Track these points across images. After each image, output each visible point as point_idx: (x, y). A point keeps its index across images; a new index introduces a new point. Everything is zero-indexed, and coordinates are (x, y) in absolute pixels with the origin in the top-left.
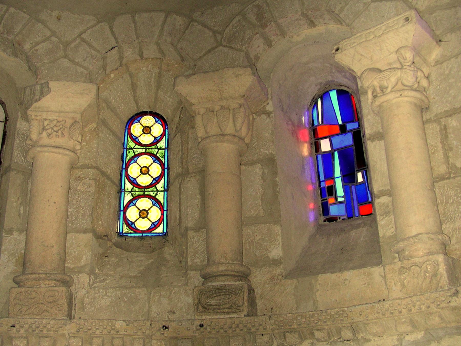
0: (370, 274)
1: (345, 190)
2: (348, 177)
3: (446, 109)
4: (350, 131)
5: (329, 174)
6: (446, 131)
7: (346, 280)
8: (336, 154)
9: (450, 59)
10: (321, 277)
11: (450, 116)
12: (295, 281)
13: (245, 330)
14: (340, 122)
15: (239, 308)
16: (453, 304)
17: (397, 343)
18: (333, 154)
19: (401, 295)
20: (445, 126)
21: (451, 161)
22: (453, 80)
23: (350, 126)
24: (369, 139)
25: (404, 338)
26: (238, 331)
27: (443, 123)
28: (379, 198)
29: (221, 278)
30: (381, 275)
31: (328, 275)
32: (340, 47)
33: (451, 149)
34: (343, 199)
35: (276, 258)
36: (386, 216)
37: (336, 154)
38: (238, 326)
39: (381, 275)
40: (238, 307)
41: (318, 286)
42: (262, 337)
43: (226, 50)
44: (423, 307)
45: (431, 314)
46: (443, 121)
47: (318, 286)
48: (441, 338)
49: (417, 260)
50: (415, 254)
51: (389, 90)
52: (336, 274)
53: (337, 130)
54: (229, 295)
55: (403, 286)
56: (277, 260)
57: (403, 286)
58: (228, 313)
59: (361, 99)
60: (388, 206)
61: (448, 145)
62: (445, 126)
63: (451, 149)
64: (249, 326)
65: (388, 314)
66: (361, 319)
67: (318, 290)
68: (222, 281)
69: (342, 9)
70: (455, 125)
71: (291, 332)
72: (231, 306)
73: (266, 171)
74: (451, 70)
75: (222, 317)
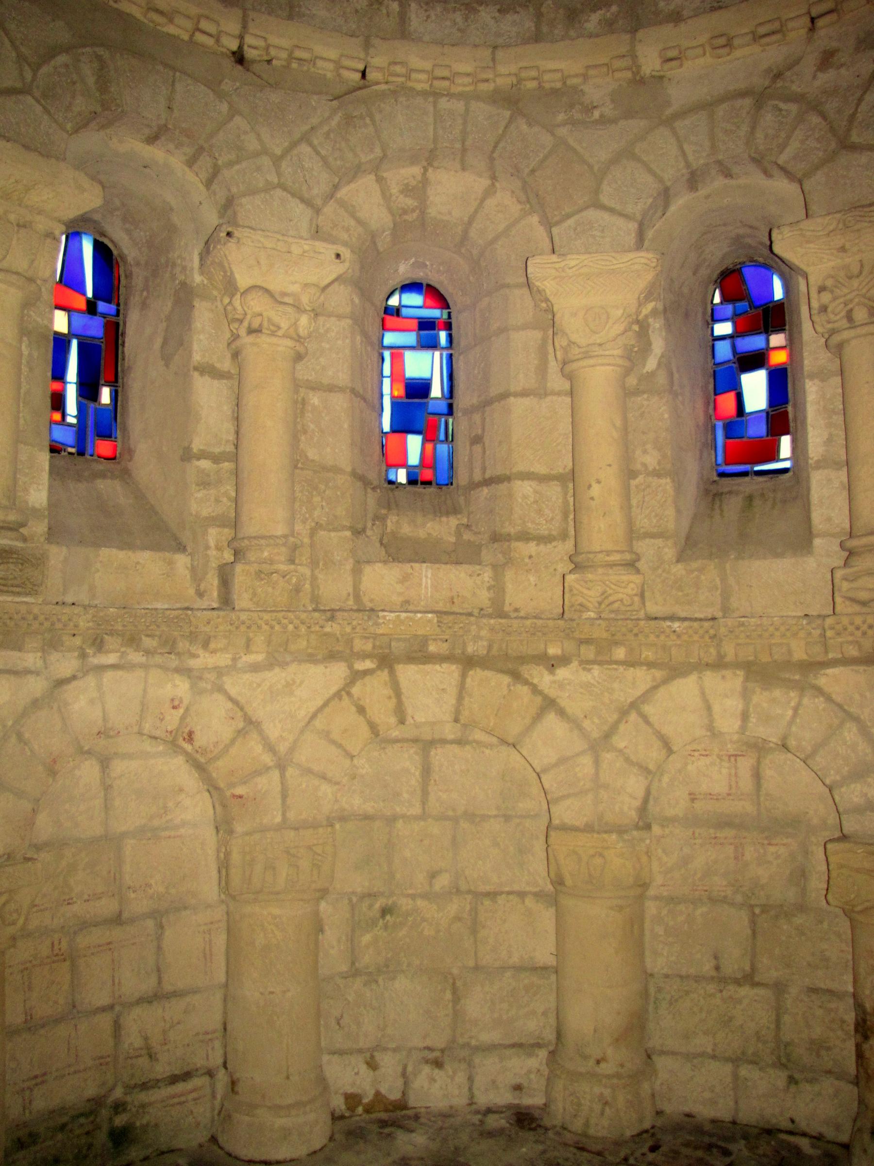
0: (171, 563)
1: (81, 408)
2: (88, 391)
3: (310, 378)
4: (104, 315)
5: (59, 373)
6: (303, 408)
7: (138, 563)
8: (74, 344)
9: (329, 316)
10: (105, 553)
11: (313, 389)
12: (64, 549)
13: (47, 624)
14: (90, 294)
15: (36, 588)
16: (328, 629)
17: (230, 663)
18: (69, 342)
19: (251, 606)
20: (303, 399)
21: (302, 446)
22: (327, 346)
23: (102, 306)
24: (196, 369)
25: (240, 658)
26: (36, 625)
27: (302, 395)
28: (199, 459)
29: (9, 533)
30: (187, 568)
31: (114, 551)
32: (236, 234)
33: (305, 432)
34: (74, 421)
35: (37, 506)
36: (204, 488)
37: (74, 344)
38: (36, 618)
39: (187, 568)
40: (35, 585)
41: (98, 565)
42: (72, 638)
43: (38, 109)
44: (291, 627)
45: (299, 636)
46: (302, 391)
47: (98, 565)
48: (287, 664)
49: (282, 567)
50: (277, 558)
51: (280, 333)
52: (124, 552)
53: (83, 305)
54: (22, 564)
55: (255, 594)
56: (40, 510)
57: (255, 594)
58: (19, 594)
59: (195, 303)
60: (208, 475)
61: (303, 425)
62: (303, 399)
63: (305, 432)
64: (54, 618)
65: (243, 628)
66: (207, 629)
67: (98, 571)
68: (12, 539)
69: (230, 164)
70: (316, 403)
71: (112, 635)
72: (23, 583)
73: (35, 354)
74: (327, 331)
75: (10, 599)
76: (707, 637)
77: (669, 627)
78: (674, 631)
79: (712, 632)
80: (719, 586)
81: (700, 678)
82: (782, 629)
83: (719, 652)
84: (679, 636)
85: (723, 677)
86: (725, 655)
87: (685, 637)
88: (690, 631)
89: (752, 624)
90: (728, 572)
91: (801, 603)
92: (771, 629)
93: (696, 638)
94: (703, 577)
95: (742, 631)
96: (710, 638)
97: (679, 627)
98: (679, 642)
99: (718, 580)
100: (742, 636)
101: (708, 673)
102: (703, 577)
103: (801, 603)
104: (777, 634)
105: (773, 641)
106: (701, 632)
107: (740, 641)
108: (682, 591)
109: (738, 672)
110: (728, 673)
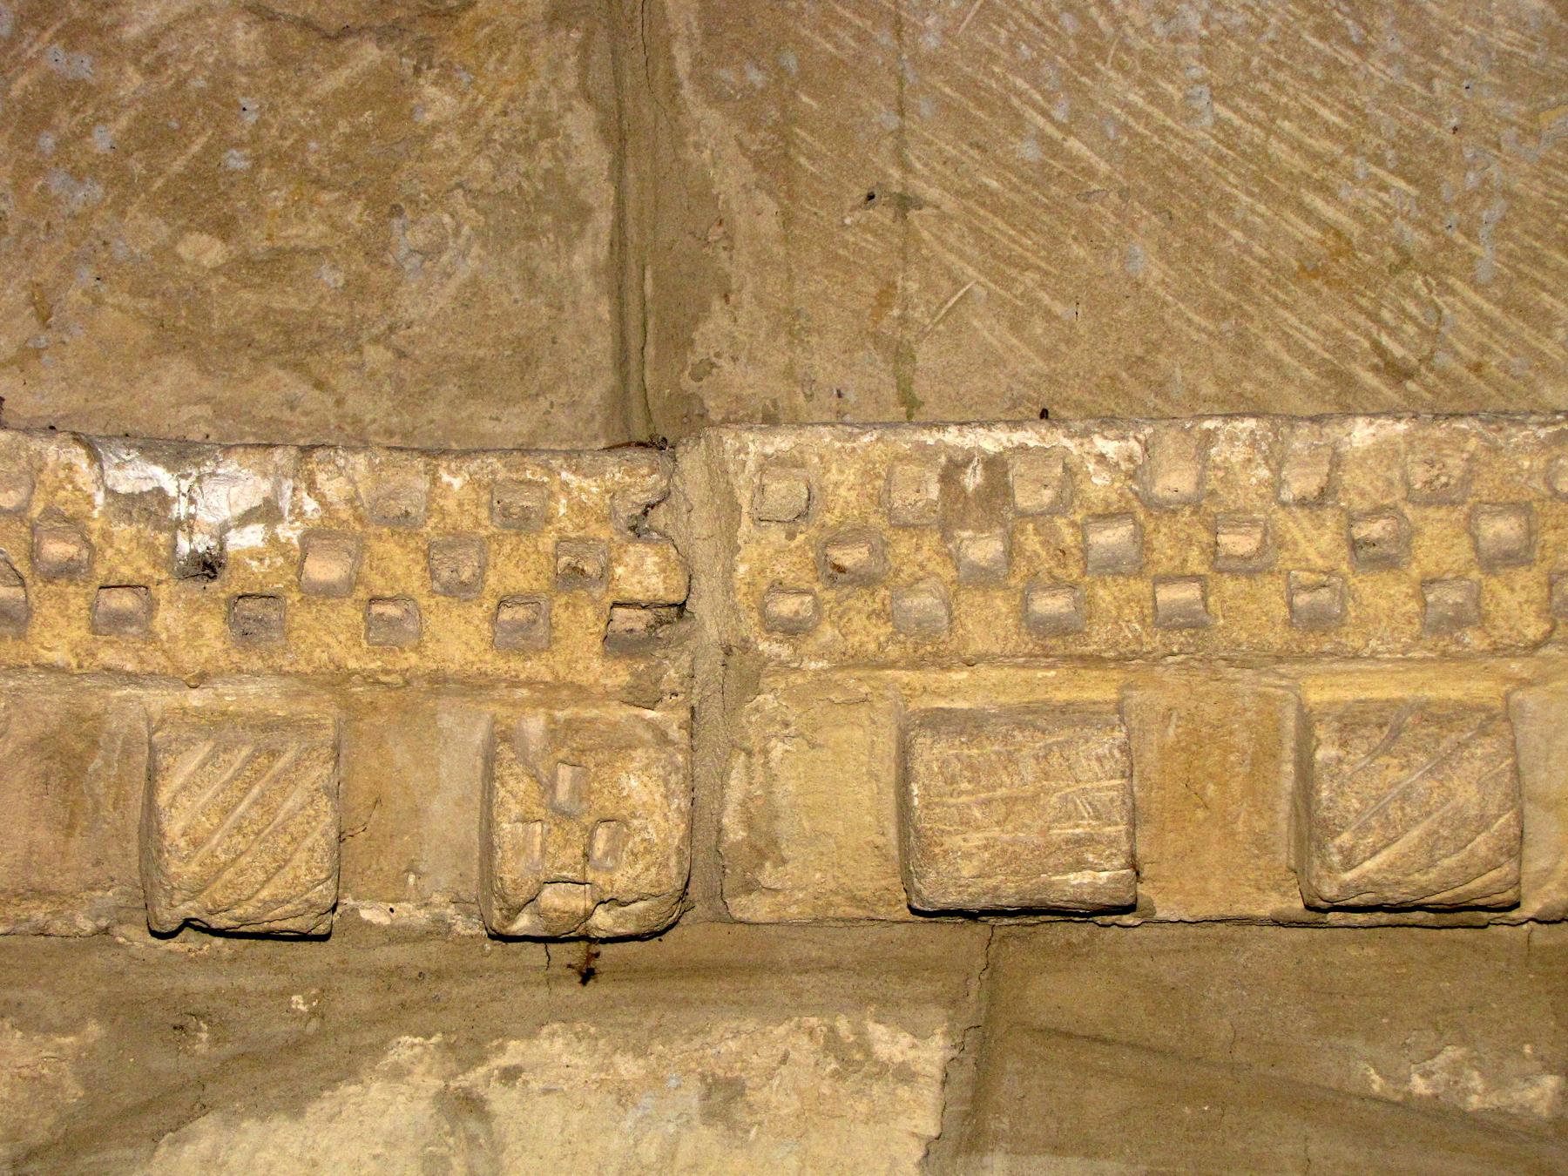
76: (580, 626)
77: (149, 508)
78: (208, 567)
79: (643, 573)
80: (599, 194)
81: (466, 1106)
82: (1439, 544)
83: (698, 821)
84: (255, 618)
85: (724, 1098)
86: (765, 849)
87: (330, 638)
88: (398, 564)
89: (1099, 484)
90: (683, 60)
91: (1397, 372)
92: (1315, 543)
93: (458, 639)
94: (437, 101)
95: (983, 579)
96: (616, 645)
97: (267, 513)
98: (255, 694)
99: (580, 125)
100: (988, 622)
101: (556, 1052)
102: (437, 101)
103: (1397, 372)
104: (1384, 595)
105: (1325, 690)
106: (515, 570)
107: (961, 689)
108: (224, 228)
109: (890, 1043)
110: (777, 1050)
